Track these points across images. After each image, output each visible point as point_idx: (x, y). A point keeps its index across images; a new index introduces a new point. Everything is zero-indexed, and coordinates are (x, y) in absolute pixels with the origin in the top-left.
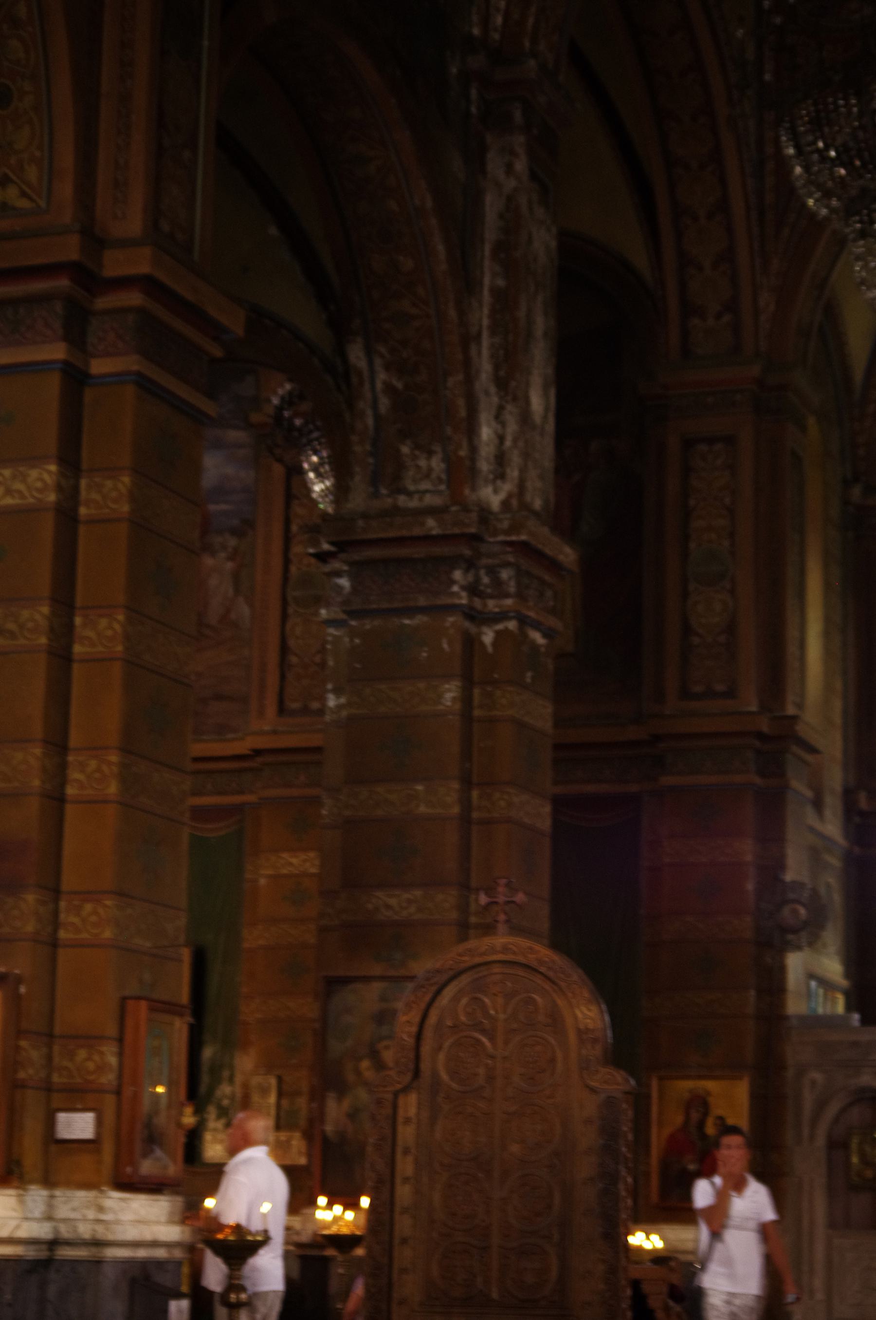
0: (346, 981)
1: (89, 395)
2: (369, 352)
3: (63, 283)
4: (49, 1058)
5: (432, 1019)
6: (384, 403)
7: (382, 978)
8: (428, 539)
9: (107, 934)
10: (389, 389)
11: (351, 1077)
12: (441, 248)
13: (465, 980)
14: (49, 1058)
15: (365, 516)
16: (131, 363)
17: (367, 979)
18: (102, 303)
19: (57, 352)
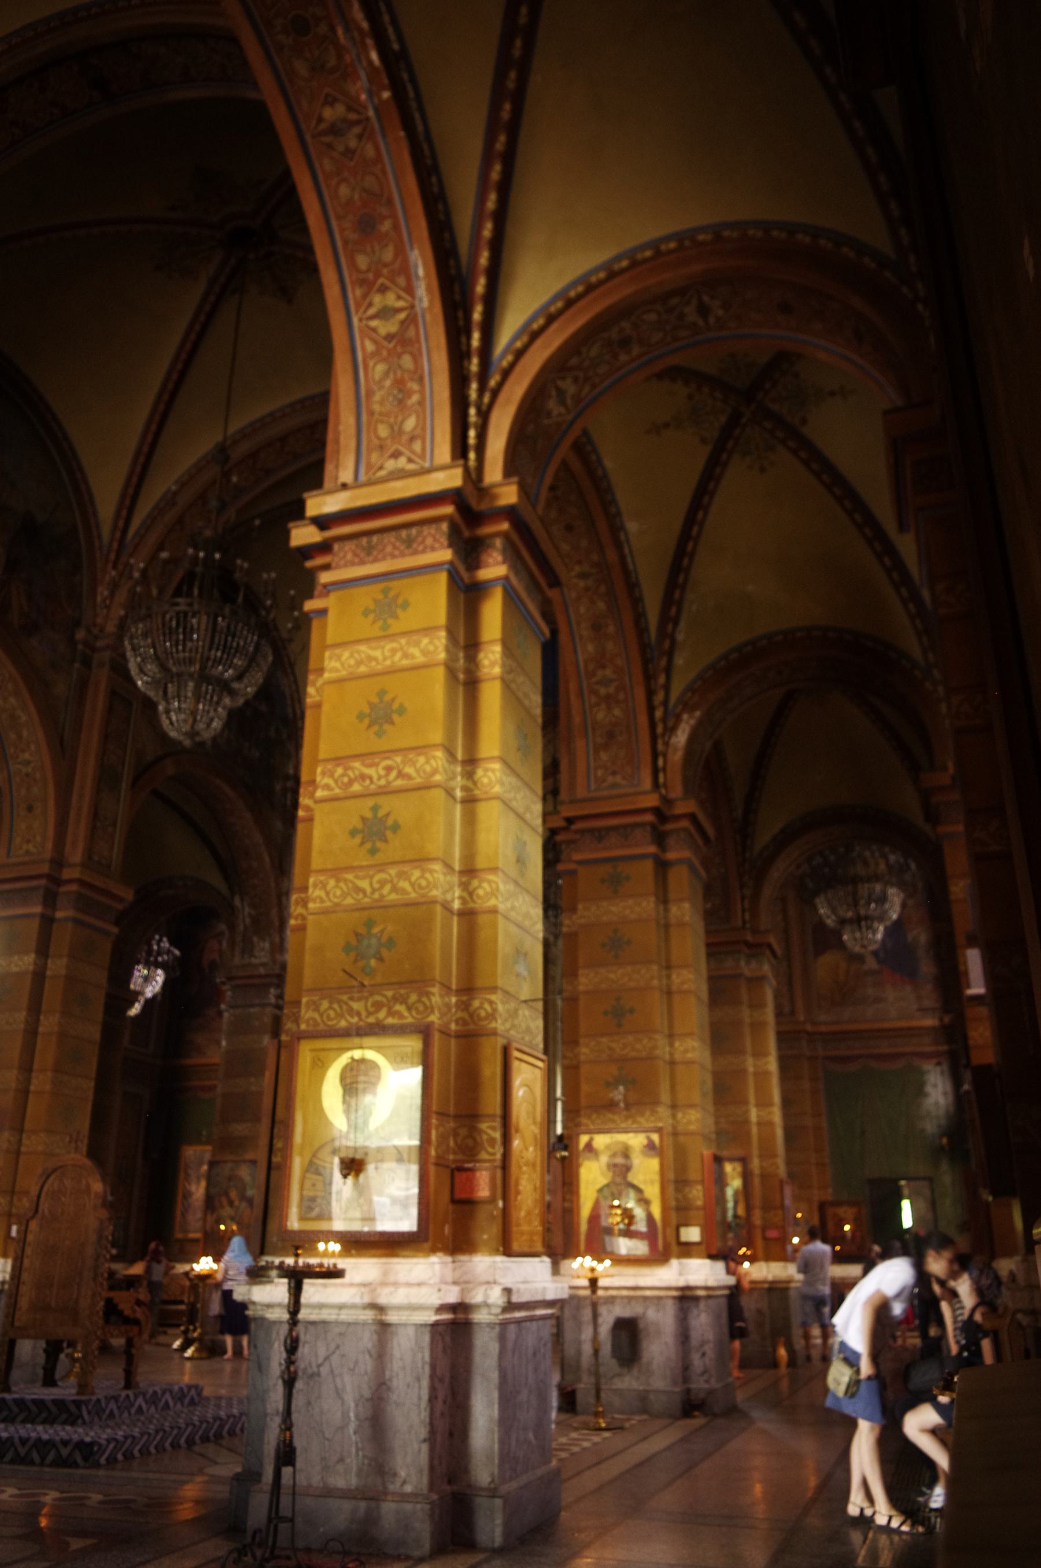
1: (55, 926)
2: (242, 900)
3: (43, 882)
5: (46, 1188)
6: (248, 921)
8: (260, 976)
12: (267, 859)
14: (11, 1202)
17: (225, 1162)
18: (63, 889)
19: (38, 909)
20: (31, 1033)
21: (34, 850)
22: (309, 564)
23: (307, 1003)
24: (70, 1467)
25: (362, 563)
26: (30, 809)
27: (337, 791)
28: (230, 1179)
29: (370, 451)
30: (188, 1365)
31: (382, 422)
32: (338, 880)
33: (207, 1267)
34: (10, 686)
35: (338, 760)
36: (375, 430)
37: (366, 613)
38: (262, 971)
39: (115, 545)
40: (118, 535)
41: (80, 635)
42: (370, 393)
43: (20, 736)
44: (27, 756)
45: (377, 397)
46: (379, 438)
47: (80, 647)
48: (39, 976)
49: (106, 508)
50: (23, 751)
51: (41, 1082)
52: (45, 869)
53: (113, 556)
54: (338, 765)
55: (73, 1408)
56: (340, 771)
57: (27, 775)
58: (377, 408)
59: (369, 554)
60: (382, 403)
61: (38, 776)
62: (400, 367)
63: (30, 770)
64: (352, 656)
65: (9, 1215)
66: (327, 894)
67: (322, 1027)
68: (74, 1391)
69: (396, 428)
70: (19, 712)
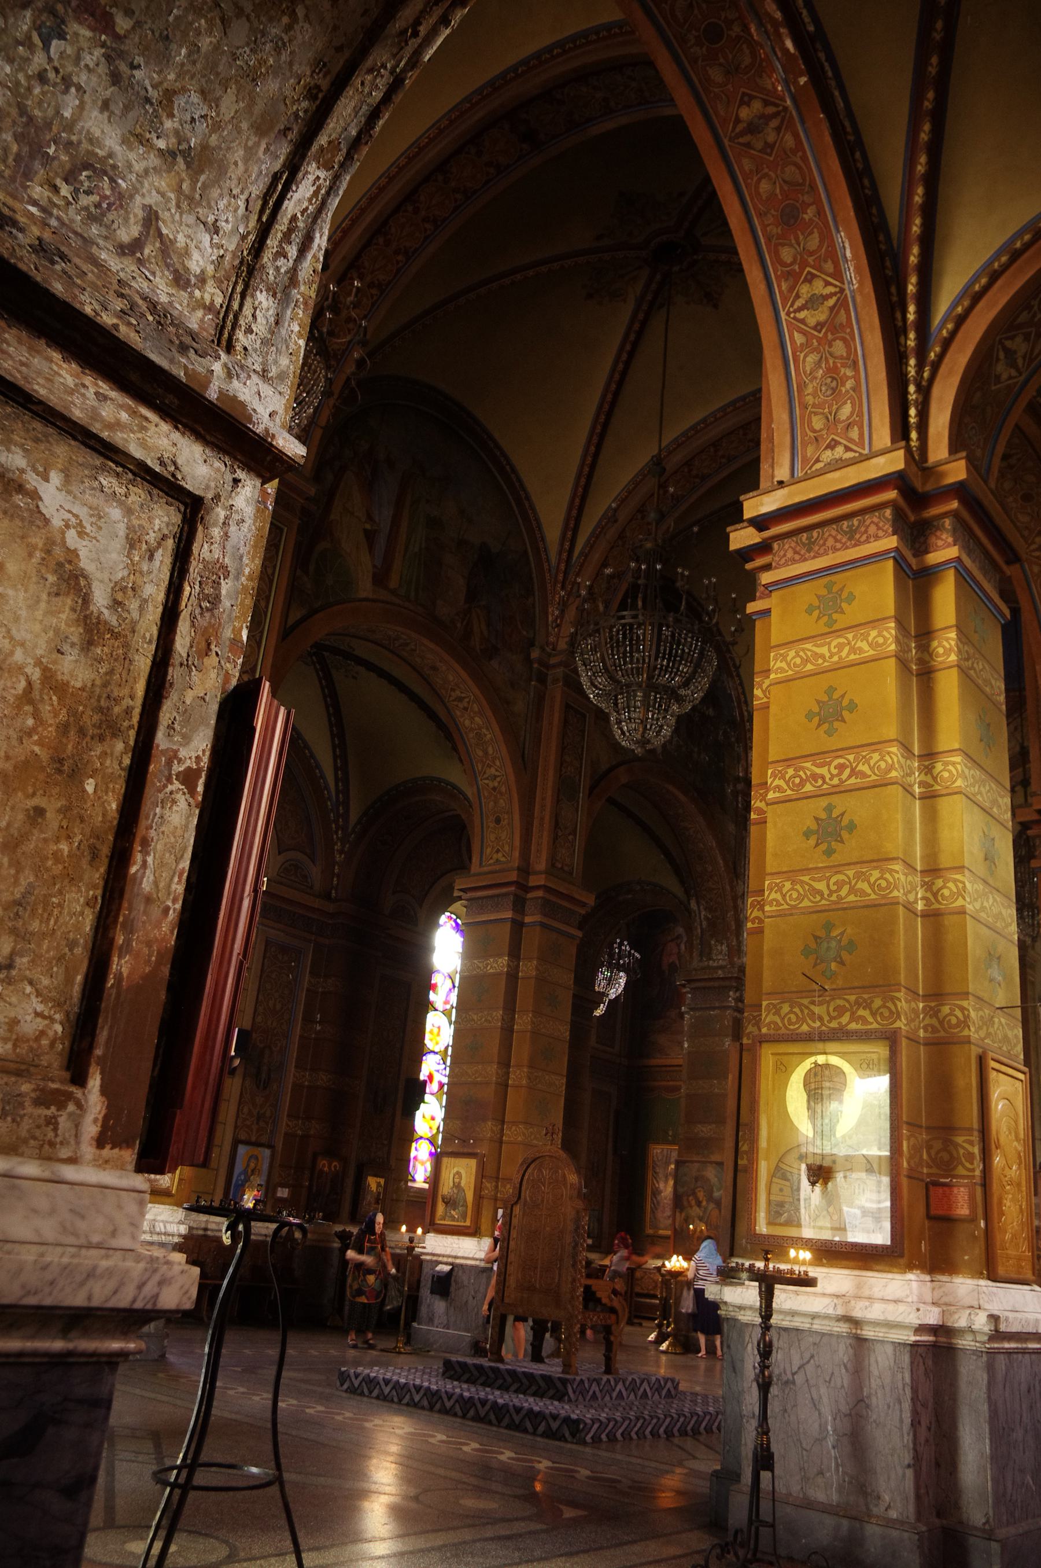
0: (685, 1162)
1: (524, 929)
2: (698, 903)
3: (512, 889)
4: (497, 1187)
5: (526, 1177)
6: (704, 923)
7: (699, 1162)
9: (520, 1139)
10: (706, 918)
11: (685, 1203)
13: (537, 1162)
14: (497, 1187)
15: (695, 970)
16: (537, 918)
17: (692, 1162)
18: (529, 896)
19: (509, 915)
20: (508, 1030)
21: (503, 859)
22: (749, 566)
23: (768, 1005)
24: (559, 1440)
25: (804, 560)
26: (498, 821)
27: (789, 792)
28: (697, 1179)
29: (805, 445)
30: (664, 1358)
31: (816, 414)
32: (793, 882)
33: (678, 1265)
34: (476, 708)
35: (788, 761)
36: (810, 422)
37: (809, 611)
38: (720, 973)
39: (563, 566)
40: (565, 555)
41: (535, 654)
42: (802, 386)
43: (486, 753)
44: (493, 771)
45: (810, 389)
46: (814, 431)
47: (536, 665)
48: (512, 977)
49: (553, 532)
50: (489, 766)
51: (518, 1076)
52: (513, 876)
53: (561, 577)
54: (789, 766)
55: (559, 1385)
56: (791, 772)
57: (494, 789)
58: (810, 400)
59: (809, 551)
60: (815, 395)
61: (503, 789)
62: (831, 354)
63: (496, 784)
64: (797, 655)
65: (496, 1199)
66: (784, 896)
67: (783, 1031)
68: (560, 1369)
69: (831, 418)
70: (484, 730)
